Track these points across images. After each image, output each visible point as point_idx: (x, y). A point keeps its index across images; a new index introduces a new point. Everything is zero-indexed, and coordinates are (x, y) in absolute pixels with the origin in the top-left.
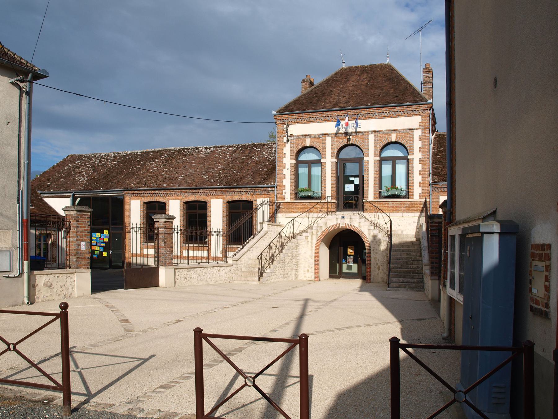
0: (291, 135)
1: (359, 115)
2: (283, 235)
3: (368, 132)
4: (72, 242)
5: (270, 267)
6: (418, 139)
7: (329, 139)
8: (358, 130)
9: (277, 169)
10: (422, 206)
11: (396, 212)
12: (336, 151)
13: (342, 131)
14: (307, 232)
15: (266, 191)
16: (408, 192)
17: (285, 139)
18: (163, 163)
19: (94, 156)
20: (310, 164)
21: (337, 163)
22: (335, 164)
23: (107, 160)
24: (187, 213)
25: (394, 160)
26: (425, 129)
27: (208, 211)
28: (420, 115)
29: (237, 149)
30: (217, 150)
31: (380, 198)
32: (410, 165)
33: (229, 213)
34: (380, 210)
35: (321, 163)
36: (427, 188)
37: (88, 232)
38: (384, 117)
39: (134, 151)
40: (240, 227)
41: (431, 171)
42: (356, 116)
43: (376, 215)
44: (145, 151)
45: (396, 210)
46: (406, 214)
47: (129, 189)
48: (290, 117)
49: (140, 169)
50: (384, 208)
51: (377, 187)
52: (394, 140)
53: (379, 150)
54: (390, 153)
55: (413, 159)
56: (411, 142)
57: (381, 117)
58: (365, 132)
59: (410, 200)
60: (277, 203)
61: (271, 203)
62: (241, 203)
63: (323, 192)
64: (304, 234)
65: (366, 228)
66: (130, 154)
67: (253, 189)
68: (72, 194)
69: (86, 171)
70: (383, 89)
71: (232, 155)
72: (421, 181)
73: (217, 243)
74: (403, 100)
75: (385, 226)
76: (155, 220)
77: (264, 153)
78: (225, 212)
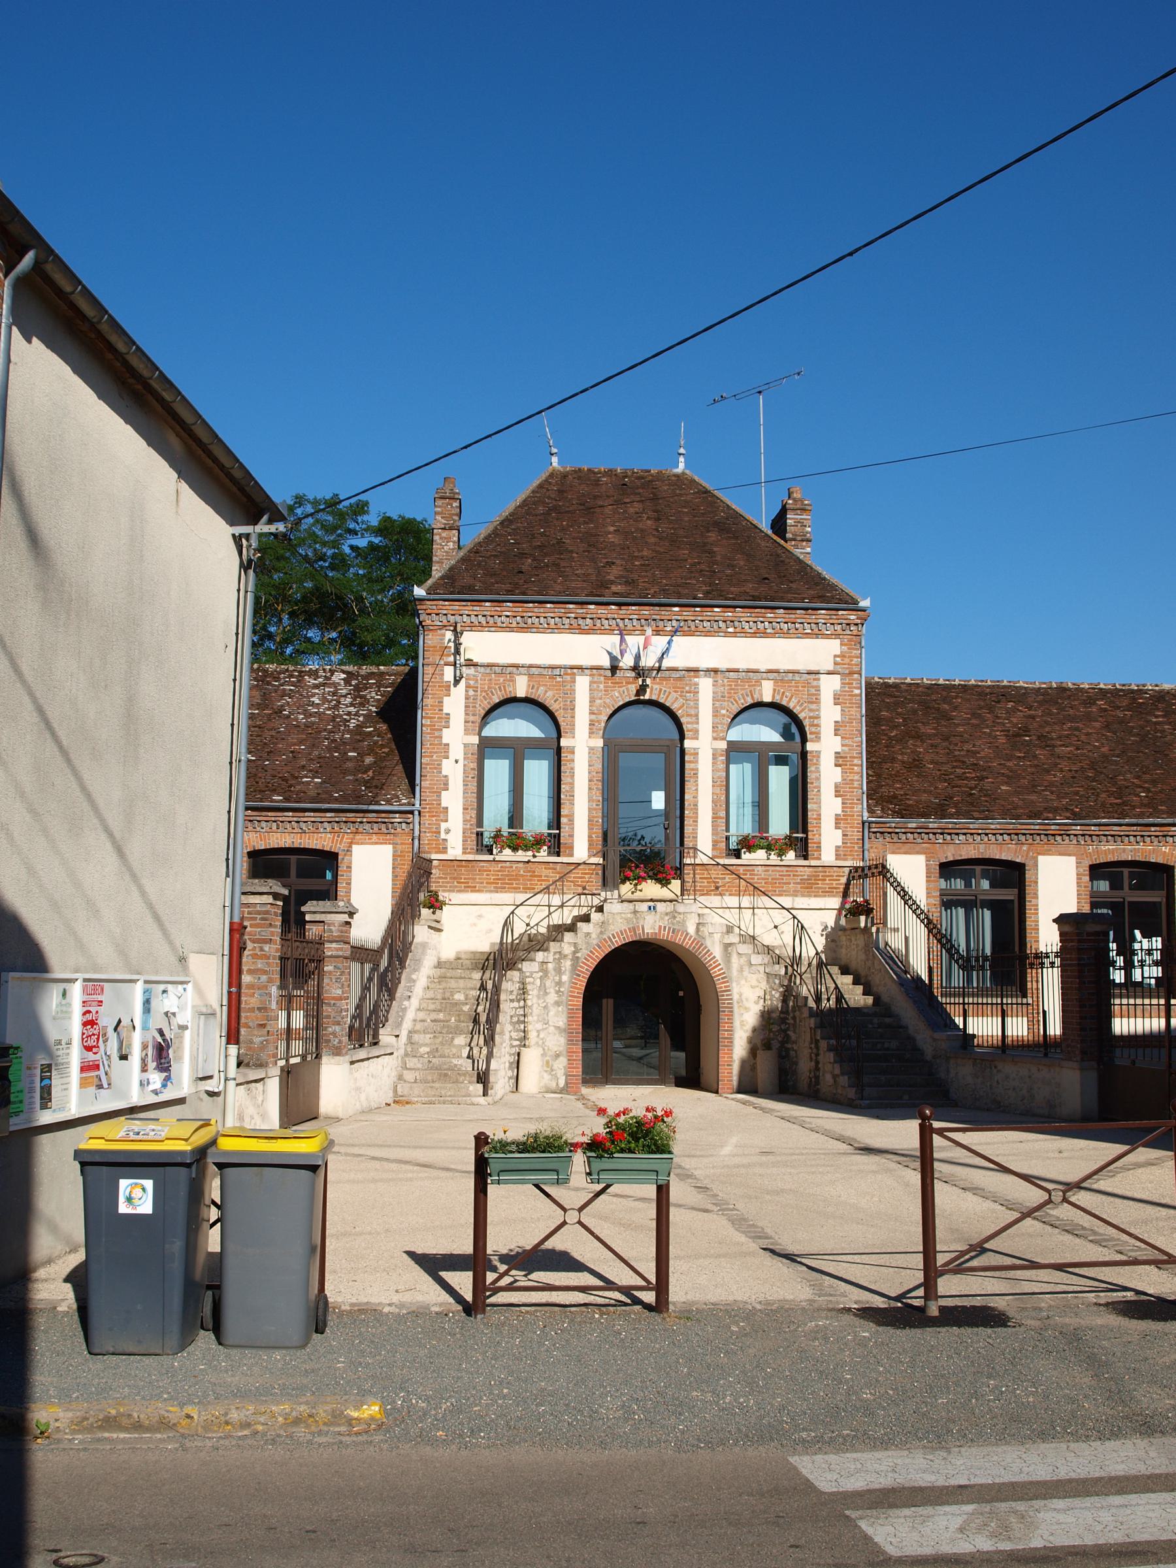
0: (470, 663)
3: (696, 670)
6: (832, 701)
7: (582, 683)
8: (666, 664)
10: (844, 880)
13: (627, 661)
14: (547, 950)
15: (382, 824)
17: (449, 673)
20: (517, 751)
26: (851, 673)
28: (837, 636)
34: (756, 890)
38: (743, 634)
43: (746, 901)
48: (467, 609)
56: (813, 707)
57: (734, 635)
58: (689, 670)
59: (813, 863)
62: (293, 858)
64: (540, 956)
65: (717, 937)
67: (343, 817)
72: (839, 812)
74: (789, 590)
76: (308, 918)
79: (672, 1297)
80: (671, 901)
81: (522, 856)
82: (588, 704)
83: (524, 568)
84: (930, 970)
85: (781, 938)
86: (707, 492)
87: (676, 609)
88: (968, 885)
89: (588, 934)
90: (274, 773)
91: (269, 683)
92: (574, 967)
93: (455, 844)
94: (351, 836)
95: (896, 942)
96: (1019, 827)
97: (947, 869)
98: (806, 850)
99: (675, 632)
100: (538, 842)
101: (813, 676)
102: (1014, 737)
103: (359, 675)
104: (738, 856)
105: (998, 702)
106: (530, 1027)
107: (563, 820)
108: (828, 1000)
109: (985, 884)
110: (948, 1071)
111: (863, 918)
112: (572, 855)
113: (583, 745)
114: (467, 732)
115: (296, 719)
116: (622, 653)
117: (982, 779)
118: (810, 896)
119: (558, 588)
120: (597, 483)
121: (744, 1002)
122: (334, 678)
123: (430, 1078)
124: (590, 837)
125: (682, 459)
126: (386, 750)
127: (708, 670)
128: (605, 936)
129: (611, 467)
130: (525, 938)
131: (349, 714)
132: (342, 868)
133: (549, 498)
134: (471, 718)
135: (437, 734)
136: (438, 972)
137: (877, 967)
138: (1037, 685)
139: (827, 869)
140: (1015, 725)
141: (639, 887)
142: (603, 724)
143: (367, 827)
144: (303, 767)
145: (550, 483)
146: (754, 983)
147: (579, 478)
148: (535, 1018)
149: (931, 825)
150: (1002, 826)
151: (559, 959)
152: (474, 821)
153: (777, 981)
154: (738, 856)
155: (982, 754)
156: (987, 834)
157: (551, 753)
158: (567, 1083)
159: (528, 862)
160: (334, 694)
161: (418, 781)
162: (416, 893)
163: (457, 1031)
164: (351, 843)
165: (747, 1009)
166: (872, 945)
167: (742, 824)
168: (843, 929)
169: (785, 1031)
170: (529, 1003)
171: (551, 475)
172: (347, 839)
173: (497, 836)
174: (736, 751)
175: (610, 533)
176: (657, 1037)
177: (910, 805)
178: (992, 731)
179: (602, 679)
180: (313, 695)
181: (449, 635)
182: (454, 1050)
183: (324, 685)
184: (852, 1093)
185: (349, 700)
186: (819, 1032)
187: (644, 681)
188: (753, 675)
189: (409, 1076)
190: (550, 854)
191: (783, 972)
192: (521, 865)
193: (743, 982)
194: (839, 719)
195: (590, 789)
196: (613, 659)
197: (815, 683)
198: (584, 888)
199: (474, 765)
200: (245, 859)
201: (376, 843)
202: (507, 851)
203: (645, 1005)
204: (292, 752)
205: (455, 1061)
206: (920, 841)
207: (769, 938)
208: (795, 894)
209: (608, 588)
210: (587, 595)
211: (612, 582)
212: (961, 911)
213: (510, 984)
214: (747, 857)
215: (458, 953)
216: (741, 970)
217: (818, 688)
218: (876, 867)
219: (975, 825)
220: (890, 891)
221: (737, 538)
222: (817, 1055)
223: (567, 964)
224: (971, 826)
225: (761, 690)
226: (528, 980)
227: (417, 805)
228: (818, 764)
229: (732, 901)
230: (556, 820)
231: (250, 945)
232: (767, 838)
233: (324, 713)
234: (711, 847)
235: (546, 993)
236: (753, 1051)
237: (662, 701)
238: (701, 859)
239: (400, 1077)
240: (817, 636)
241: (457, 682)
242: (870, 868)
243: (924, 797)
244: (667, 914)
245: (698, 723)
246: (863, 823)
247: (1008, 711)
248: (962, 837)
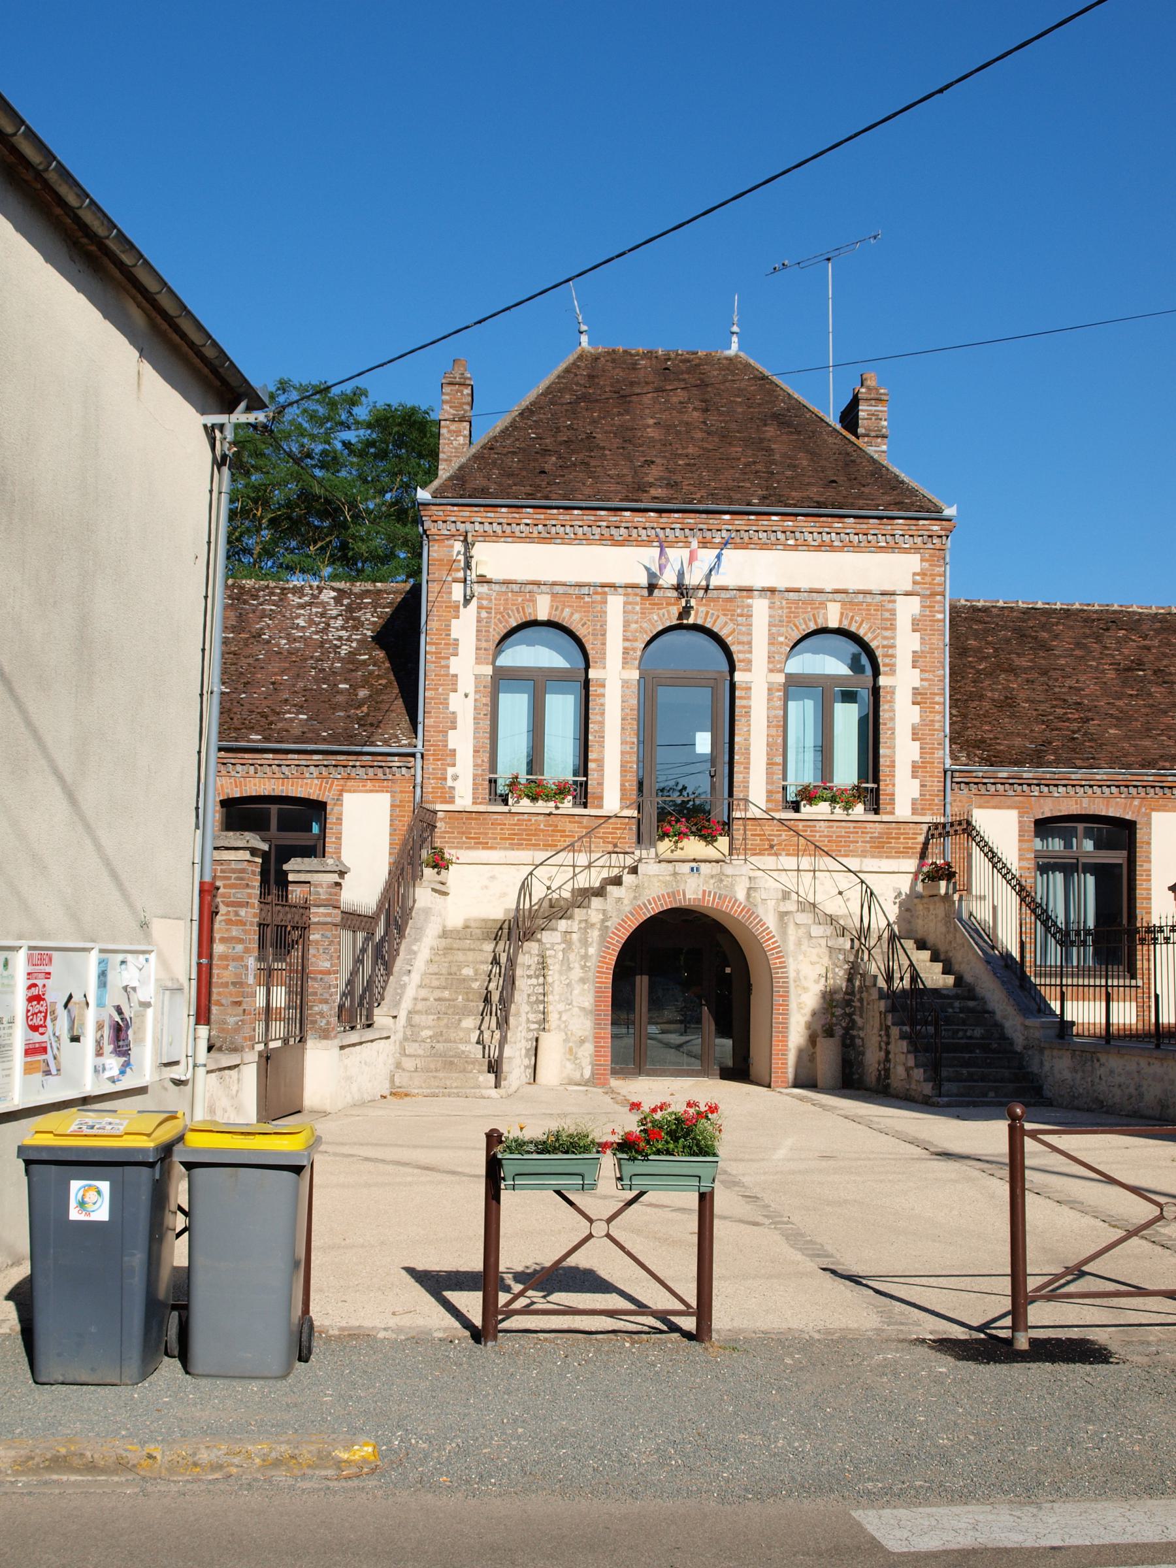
0: (483, 580)
3: (749, 590)
6: (910, 627)
8: (715, 581)
10: (921, 839)
13: (669, 578)
14: (570, 917)
17: (457, 592)
20: (538, 684)
26: (933, 594)
28: (915, 550)
32: (884, 707)
34: (818, 849)
43: (806, 862)
48: (479, 515)
56: (887, 633)
57: (795, 548)
58: (740, 590)
59: (886, 818)
62: (274, 808)
64: (563, 924)
65: (771, 904)
67: (332, 760)
72: (917, 757)
74: (860, 496)
76: (291, 877)
77: (301, 622)
79: (716, 1324)
80: (717, 862)
81: (542, 806)
82: (621, 629)
83: (547, 467)
84: (1022, 945)
85: (848, 908)
86: (764, 378)
87: (727, 517)
88: (1068, 845)
89: (619, 899)
90: (251, 707)
91: (245, 602)
92: (603, 937)
93: (464, 792)
94: (342, 782)
95: (982, 912)
96: (1130, 777)
97: (1044, 827)
98: (877, 803)
99: (725, 544)
100: (561, 791)
101: (887, 598)
102: (1125, 671)
103: (351, 593)
104: (796, 807)
105: (1108, 629)
106: (550, 1008)
107: (591, 765)
108: (902, 979)
109: (1089, 845)
110: (1042, 1063)
111: (943, 884)
112: (601, 807)
113: (615, 677)
114: (478, 661)
115: (278, 645)
116: (662, 568)
117: (1087, 720)
118: (881, 857)
119: (587, 491)
120: (634, 367)
121: (801, 981)
122: (322, 597)
123: (432, 1066)
124: (622, 785)
125: (735, 339)
126: (383, 682)
127: (763, 590)
128: (640, 903)
129: (650, 348)
130: (546, 904)
131: (340, 638)
132: (331, 819)
133: (577, 384)
135: (443, 663)
136: (444, 943)
137: (959, 941)
138: (1154, 610)
139: (902, 826)
140: (1126, 658)
141: (680, 845)
142: (639, 653)
143: (361, 771)
144: (286, 700)
145: (579, 367)
146: (815, 958)
147: (614, 361)
148: (557, 997)
149: (1025, 775)
150: (1110, 777)
151: (585, 929)
152: (486, 766)
153: (841, 957)
154: (796, 807)
155: (1087, 691)
156: (1091, 786)
157: (578, 686)
158: (593, 1074)
159: (550, 814)
160: (322, 615)
161: (420, 719)
162: (419, 849)
163: (465, 1012)
164: (342, 791)
165: (805, 989)
166: (954, 917)
167: (802, 773)
168: (920, 897)
169: (850, 1015)
170: (550, 980)
171: (580, 357)
173: (514, 783)
174: (795, 685)
175: (649, 426)
176: (699, 1021)
177: (1000, 751)
178: (1099, 664)
179: (638, 599)
180: (298, 617)
181: (458, 546)
182: (461, 1034)
183: (311, 604)
184: (928, 1089)
185: (339, 622)
186: (890, 1017)
187: (687, 602)
189: (409, 1064)
190: (575, 805)
191: (848, 945)
192: (541, 818)
193: (801, 957)
194: (917, 648)
195: (623, 729)
196: (651, 575)
197: (890, 606)
198: (615, 846)
199: (487, 700)
200: (218, 808)
201: (371, 791)
202: (525, 802)
203: (685, 980)
204: (273, 683)
205: (462, 1047)
206: (1011, 793)
207: (833, 906)
208: (864, 854)
209: (646, 492)
210: (621, 500)
211: (651, 485)
212: (1060, 876)
213: (528, 957)
214: (807, 810)
215: (466, 920)
216: (799, 943)
217: (893, 612)
218: (960, 824)
219: (1077, 775)
220: (976, 851)
221: (799, 433)
222: (888, 1043)
223: (595, 934)
224: (1073, 776)
225: (825, 615)
226: (548, 953)
227: (420, 747)
228: (892, 701)
229: (789, 862)
230: (583, 767)
231: (223, 909)
232: (831, 788)
233: (311, 638)
234: (765, 799)
235: (570, 969)
236: (812, 1039)
237: (708, 625)
238: (754, 812)
239: (398, 1066)
241: (467, 601)
242: (952, 825)
243: (1018, 741)
244: (712, 877)
245: (751, 652)
246: (945, 772)
247: (1119, 641)
248: (1061, 789)
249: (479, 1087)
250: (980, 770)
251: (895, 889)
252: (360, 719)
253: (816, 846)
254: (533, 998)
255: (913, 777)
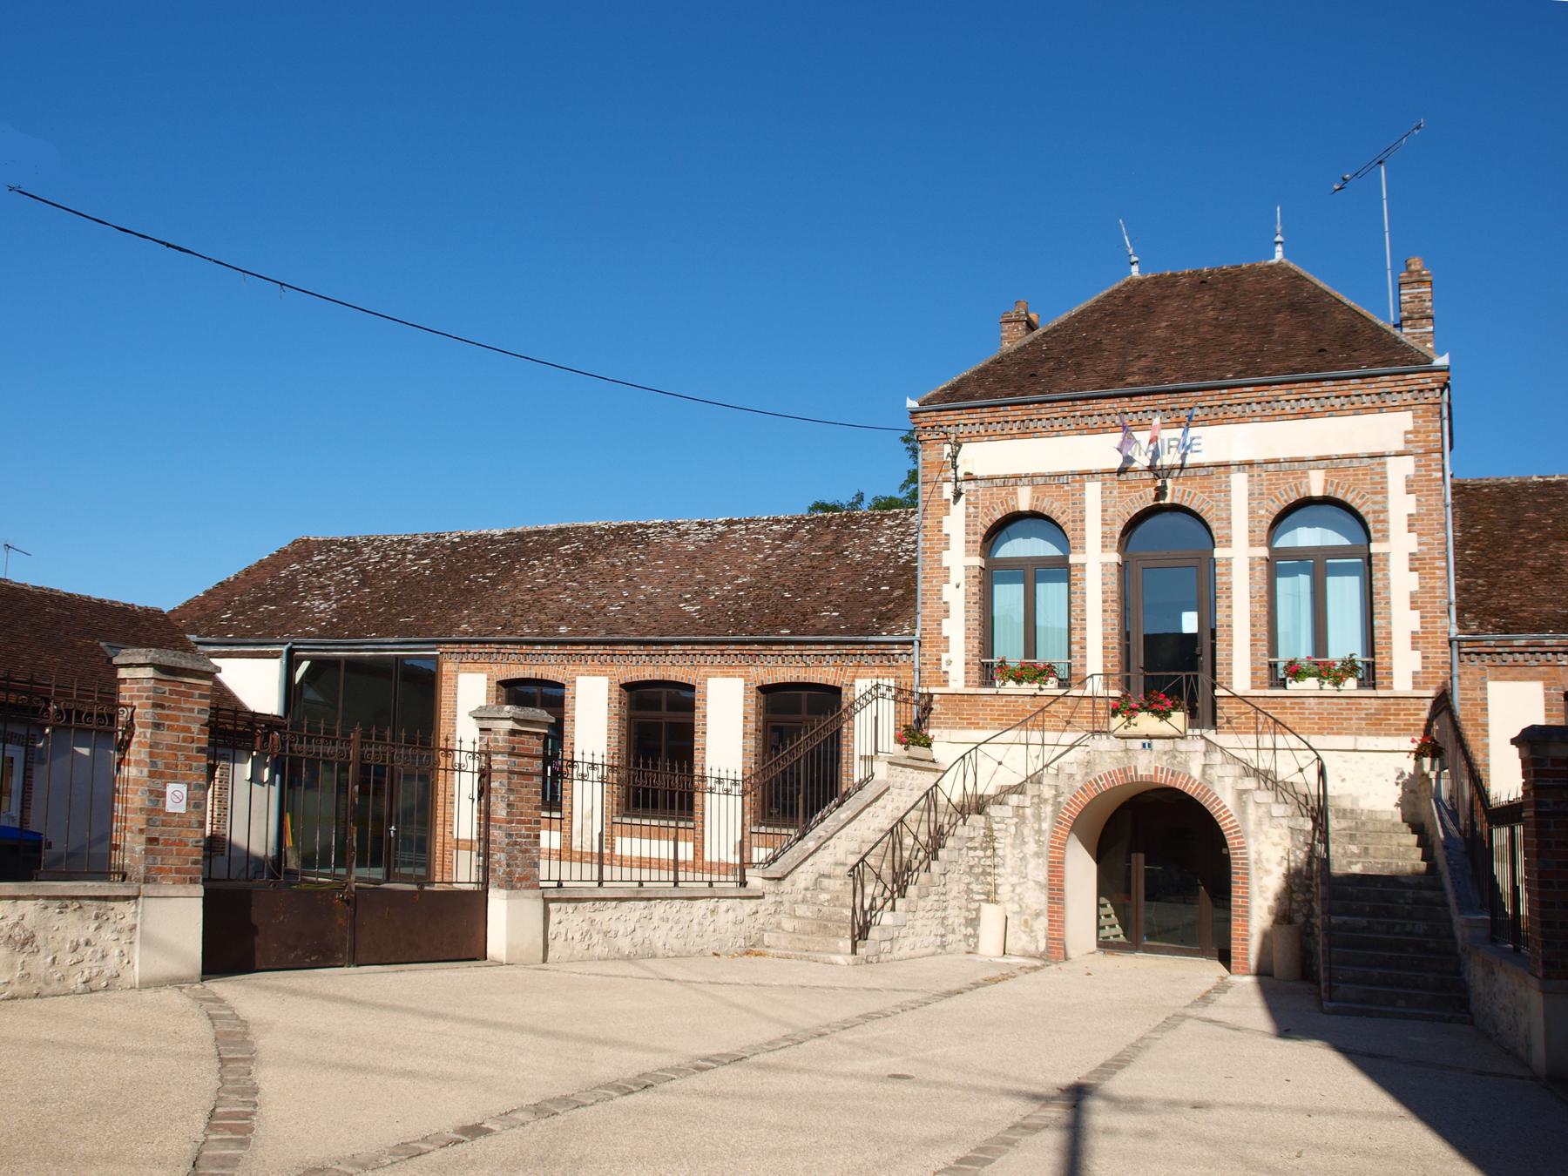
1: (1197, 411)
2: (942, 800)
3: (1227, 465)
4: (136, 781)
5: (893, 909)
6: (1404, 489)
7: (1093, 490)
8: (1190, 460)
9: (921, 586)
10: (1425, 715)
11: (1331, 732)
12: (1118, 528)
13: (1142, 461)
15: (884, 654)
16: (1371, 667)
18: (566, 565)
19: (369, 542)
20: (1031, 573)
21: (1123, 568)
22: (1114, 569)
23: (404, 554)
24: (630, 719)
25: (1317, 565)
26: (1428, 452)
27: (698, 714)
28: (1407, 407)
29: (796, 529)
30: (735, 532)
31: (1272, 686)
32: (1377, 575)
33: (766, 722)
34: (1279, 726)
35: (1068, 566)
36: (1440, 655)
37: (200, 750)
39: (484, 532)
40: (801, 769)
41: (1453, 597)
42: (1183, 414)
43: (1267, 740)
44: (519, 529)
45: (1331, 725)
46: (1366, 742)
47: (454, 637)
49: (494, 582)
50: (1288, 719)
51: (1263, 648)
52: (1317, 491)
53: (1266, 523)
54: (1306, 536)
55: (1386, 555)
56: (1379, 498)
58: (1217, 466)
60: (922, 695)
61: (902, 695)
62: (804, 693)
63: (1076, 661)
64: (1014, 799)
65: (1229, 781)
66: (474, 538)
67: (844, 649)
68: (284, 649)
69: (338, 584)
70: (1272, 332)
71: (780, 547)
72: (1417, 628)
73: (723, 817)
74: (1346, 360)
75: (1297, 779)
77: (882, 540)
78: (752, 718)
81: (1027, 688)
89: (1071, 776)
92: (1056, 812)
99: (1189, 422)
134: (972, 538)
139: (1402, 701)
146: (1276, 839)
149: (1547, 642)
152: (976, 651)
165: (1268, 872)
169: (1309, 901)
172: (849, 672)
188: (1301, 463)
189: (788, 924)
190: (1060, 686)
191: (1309, 825)
193: (1262, 838)
194: (1413, 511)
197: (1379, 469)
202: (1011, 683)
208: (1359, 732)
214: (1294, 687)
216: (1260, 823)
223: (1048, 810)
226: (995, 826)
228: (1385, 569)
237: (1186, 504)
240: (1380, 410)
246: (1450, 642)
249: (838, 952)
250: (1491, 639)
251: (1397, 769)
252: (881, 613)
253: (1276, 721)
254: (978, 870)
255: (1414, 649)
